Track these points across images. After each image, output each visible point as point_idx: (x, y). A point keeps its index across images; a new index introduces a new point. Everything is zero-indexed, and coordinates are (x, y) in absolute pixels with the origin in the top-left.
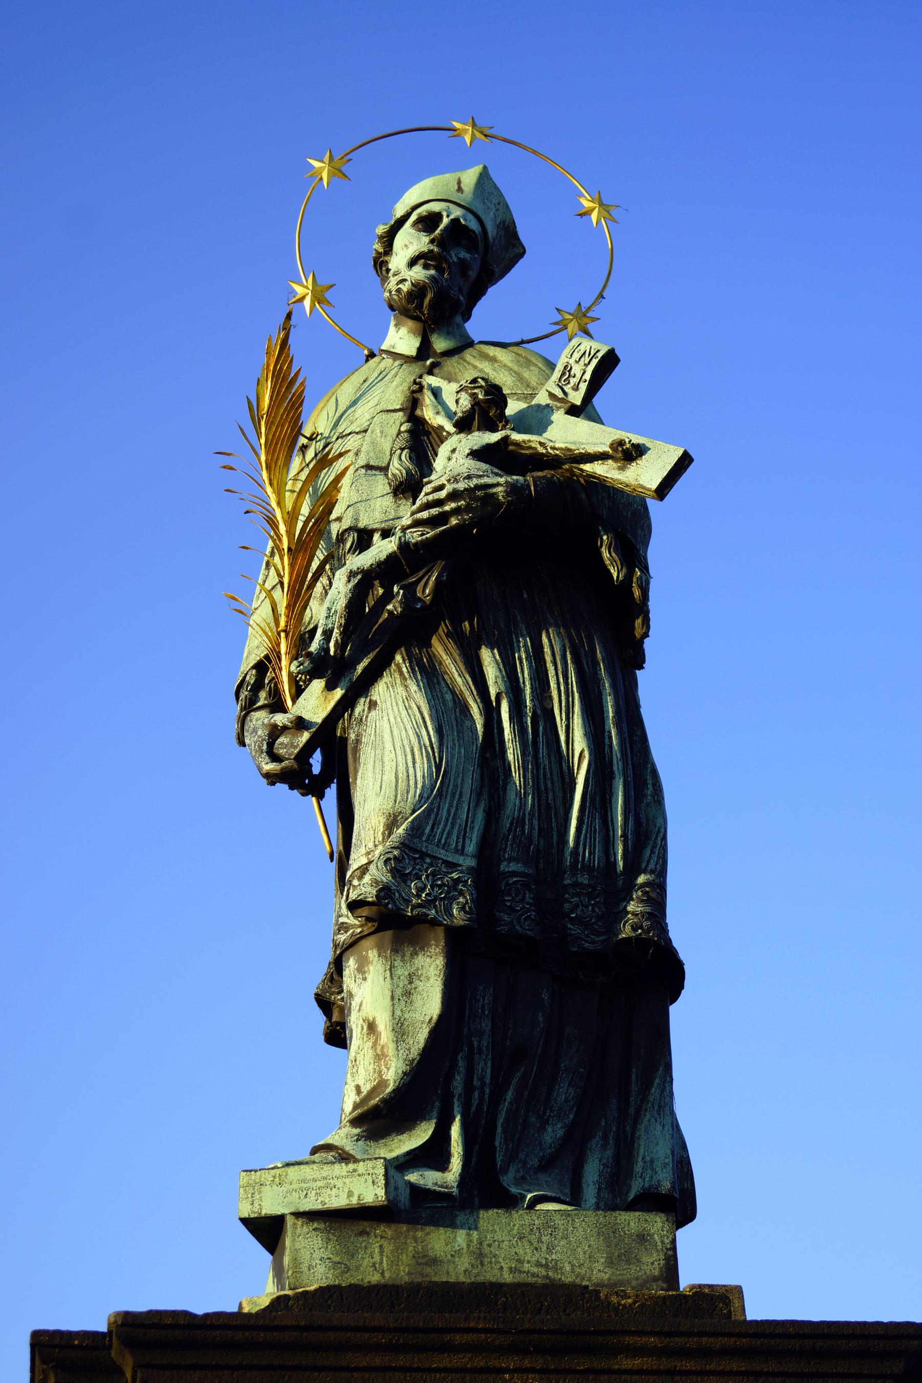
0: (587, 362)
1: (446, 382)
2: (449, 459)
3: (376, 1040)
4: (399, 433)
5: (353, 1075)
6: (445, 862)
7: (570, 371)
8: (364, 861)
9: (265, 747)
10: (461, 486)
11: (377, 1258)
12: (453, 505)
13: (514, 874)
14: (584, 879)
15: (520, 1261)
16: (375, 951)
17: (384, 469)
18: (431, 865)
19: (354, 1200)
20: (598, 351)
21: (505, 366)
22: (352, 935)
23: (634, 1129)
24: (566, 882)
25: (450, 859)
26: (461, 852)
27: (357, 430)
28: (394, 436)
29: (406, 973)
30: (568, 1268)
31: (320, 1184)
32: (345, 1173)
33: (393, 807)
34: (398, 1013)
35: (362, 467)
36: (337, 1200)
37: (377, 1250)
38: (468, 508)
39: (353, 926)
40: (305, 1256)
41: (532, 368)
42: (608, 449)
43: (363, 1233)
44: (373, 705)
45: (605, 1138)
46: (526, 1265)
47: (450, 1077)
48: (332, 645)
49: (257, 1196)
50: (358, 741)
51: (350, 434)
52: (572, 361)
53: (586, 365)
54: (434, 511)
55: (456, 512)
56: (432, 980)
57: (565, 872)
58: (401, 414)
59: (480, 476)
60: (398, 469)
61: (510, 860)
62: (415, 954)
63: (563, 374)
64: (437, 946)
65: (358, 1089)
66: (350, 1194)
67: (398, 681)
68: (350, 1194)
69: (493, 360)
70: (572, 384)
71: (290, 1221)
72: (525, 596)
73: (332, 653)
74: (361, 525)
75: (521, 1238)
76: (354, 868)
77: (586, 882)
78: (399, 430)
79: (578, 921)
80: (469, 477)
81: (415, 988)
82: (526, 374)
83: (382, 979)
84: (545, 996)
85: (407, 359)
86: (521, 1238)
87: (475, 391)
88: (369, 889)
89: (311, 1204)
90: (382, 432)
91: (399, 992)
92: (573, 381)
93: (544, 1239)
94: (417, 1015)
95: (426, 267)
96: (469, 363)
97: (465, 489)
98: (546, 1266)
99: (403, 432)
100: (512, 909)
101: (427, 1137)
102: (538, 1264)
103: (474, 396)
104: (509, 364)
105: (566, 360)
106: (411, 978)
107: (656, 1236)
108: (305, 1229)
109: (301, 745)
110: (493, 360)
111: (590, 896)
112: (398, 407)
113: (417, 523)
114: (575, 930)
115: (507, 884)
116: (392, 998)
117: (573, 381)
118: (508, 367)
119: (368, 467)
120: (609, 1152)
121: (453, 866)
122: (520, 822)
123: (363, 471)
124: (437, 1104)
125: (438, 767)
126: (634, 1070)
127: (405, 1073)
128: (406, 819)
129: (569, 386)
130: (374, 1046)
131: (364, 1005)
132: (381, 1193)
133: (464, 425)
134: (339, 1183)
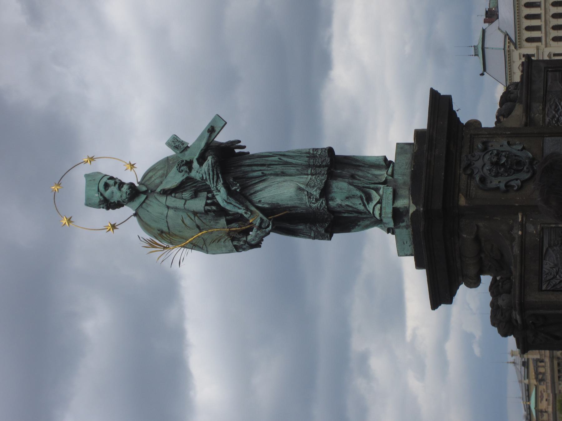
0: (176, 140)
1: (162, 185)
2: (199, 173)
3: (350, 197)
4: (175, 197)
5: (356, 205)
6: (310, 179)
7: (177, 146)
8: (307, 197)
9: (264, 230)
10: (211, 169)
11: (403, 192)
12: (215, 171)
13: (311, 171)
14: (312, 161)
15: (405, 168)
16: (330, 195)
17: (186, 200)
18: (311, 182)
19: (391, 193)
20: (174, 137)
21: (154, 175)
22: (325, 201)
23: (368, 165)
24: (312, 164)
25: (309, 179)
26: (307, 178)
27: (167, 211)
28: (175, 198)
29: (336, 189)
30: (407, 161)
31: (387, 200)
32: (385, 195)
33: (296, 188)
34: (345, 191)
35: (184, 206)
36: (391, 197)
37: (402, 192)
38: (216, 168)
39: (322, 201)
40: (401, 204)
41: (157, 167)
42: (209, 134)
43: (397, 194)
44: (260, 201)
45: (369, 170)
46: (406, 167)
47: (359, 186)
48: (243, 208)
49: (388, 213)
50: (268, 204)
51: (167, 213)
52: (173, 145)
53: (177, 140)
54: (215, 176)
55: (217, 171)
56: (339, 184)
57: (310, 164)
58: (168, 197)
59: (209, 164)
60: (189, 195)
61: (307, 171)
62: (332, 187)
63: (177, 148)
64: (331, 182)
65: (360, 204)
66: (390, 194)
67: (255, 195)
68: (390, 194)
69: (151, 178)
70: (181, 145)
71: (394, 206)
72: (233, 168)
73: (244, 208)
74: (203, 205)
75: (400, 168)
76: (307, 200)
77: (313, 160)
78: (174, 197)
79: (322, 162)
80: (209, 166)
81: (340, 187)
82: (159, 168)
83: (336, 194)
84: (339, 171)
85: (146, 198)
86: (400, 168)
87: (182, 165)
88: (317, 191)
89: (391, 202)
90: (173, 202)
91: (340, 191)
92: (180, 145)
93: (401, 164)
94: (346, 188)
95: (122, 187)
96: (151, 183)
97: (212, 168)
98: (407, 164)
99: (175, 196)
100: (321, 171)
101: (373, 190)
102: (406, 165)
103: (183, 165)
104: (154, 173)
105: (173, 147)
106: (337, 188)
107: (402, 146)
108: (396, 203)
109: (267, 219)
110: (151, 178)
111: (316, 160)
112: (165, 198)
113: (217, 182)
114: (324, 164)
115: (314, 172)
116: (342, 192)
117: (180, 145)
118: (155, 173)
119: (185, 204)
120: (373, 169)
121: (311, 179)
122: (298, 170)
123: (185, 205)
124: (365, 189)
125: (284, 181)
126: (354, 163)
127: (359, 191)
128: (299, 186)
129: (181, 146)
130: (351, 197)
131: (342, 199)
132: (391, 188)
133: (190, 169)
134: (388, 196)
